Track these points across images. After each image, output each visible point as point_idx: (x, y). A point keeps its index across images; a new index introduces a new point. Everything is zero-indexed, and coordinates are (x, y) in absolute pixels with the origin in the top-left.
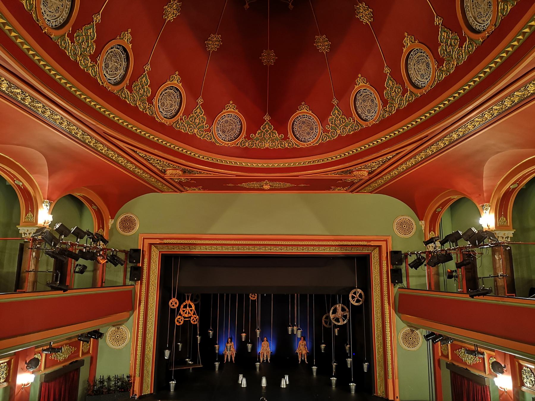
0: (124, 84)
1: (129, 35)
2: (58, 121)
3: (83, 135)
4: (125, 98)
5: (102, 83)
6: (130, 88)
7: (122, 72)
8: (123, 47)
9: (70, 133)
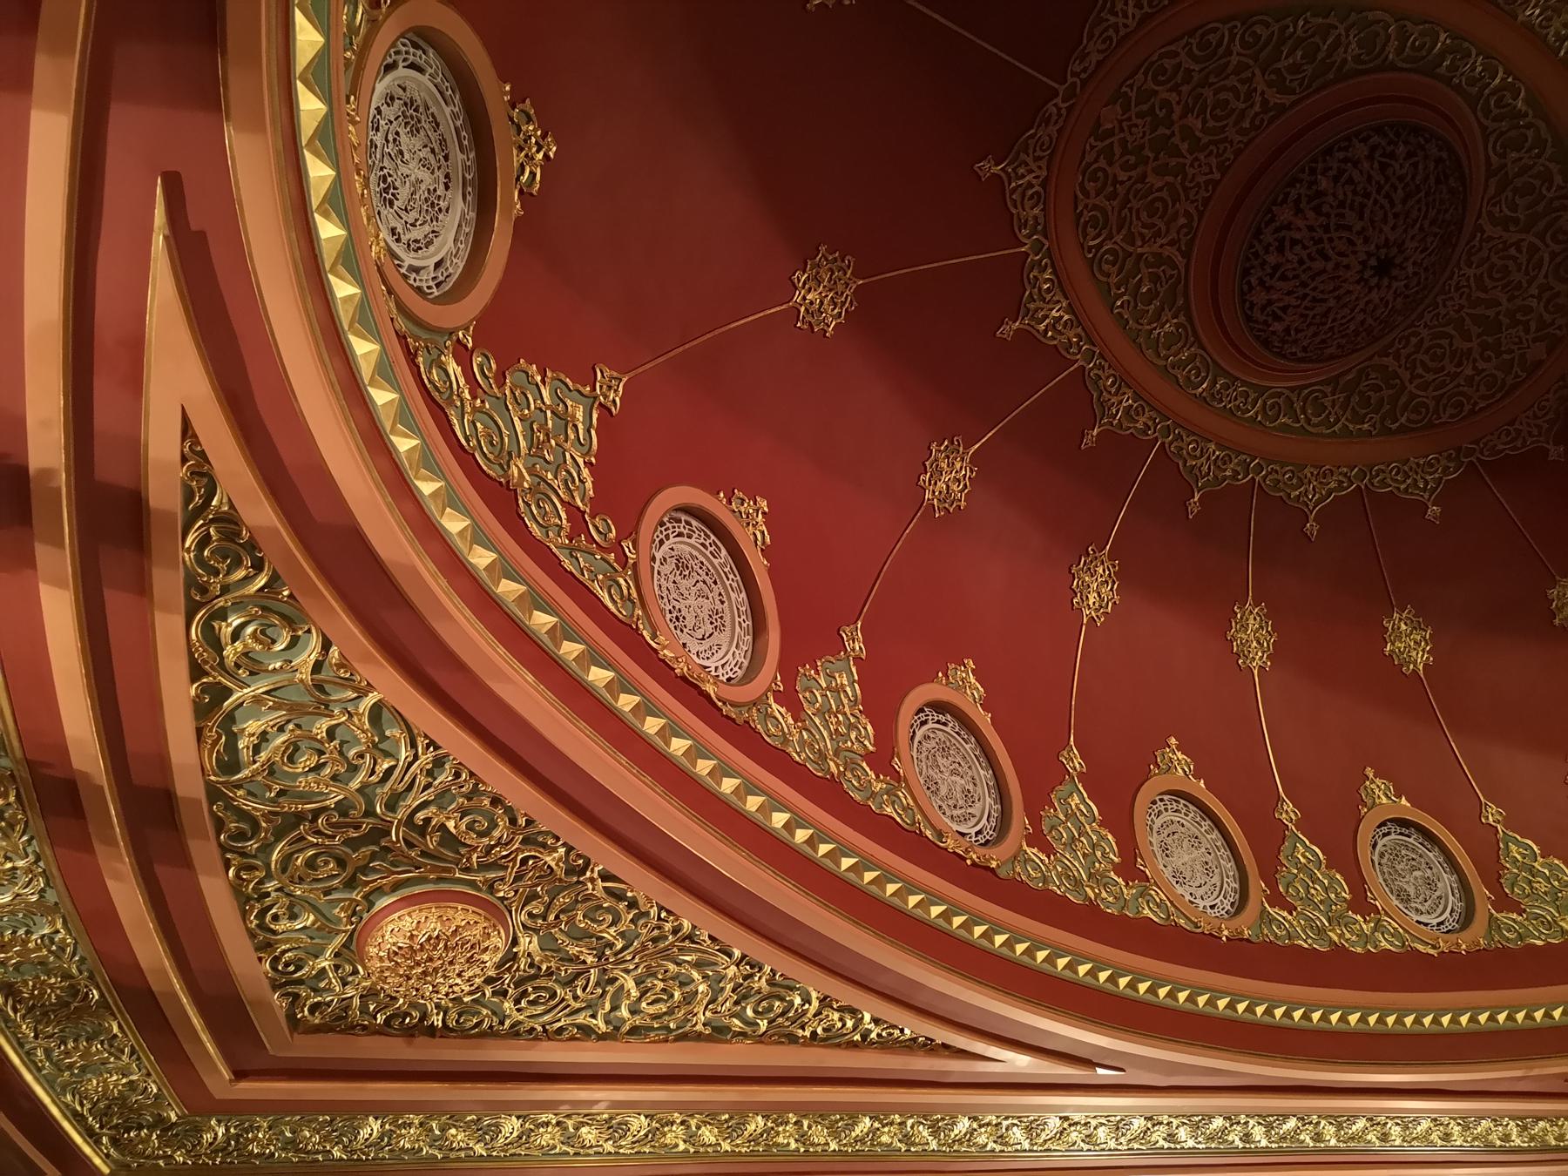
0: (1484, 908)
1: (1378, 781)
2: (1434, 1137)
3: (1524, 1128)
4: (1521, 937)
5: (1434, 947)
6: (1504, 902)
7: (1447, 880)
8: (1390, 820)
9: (1490, 1148)
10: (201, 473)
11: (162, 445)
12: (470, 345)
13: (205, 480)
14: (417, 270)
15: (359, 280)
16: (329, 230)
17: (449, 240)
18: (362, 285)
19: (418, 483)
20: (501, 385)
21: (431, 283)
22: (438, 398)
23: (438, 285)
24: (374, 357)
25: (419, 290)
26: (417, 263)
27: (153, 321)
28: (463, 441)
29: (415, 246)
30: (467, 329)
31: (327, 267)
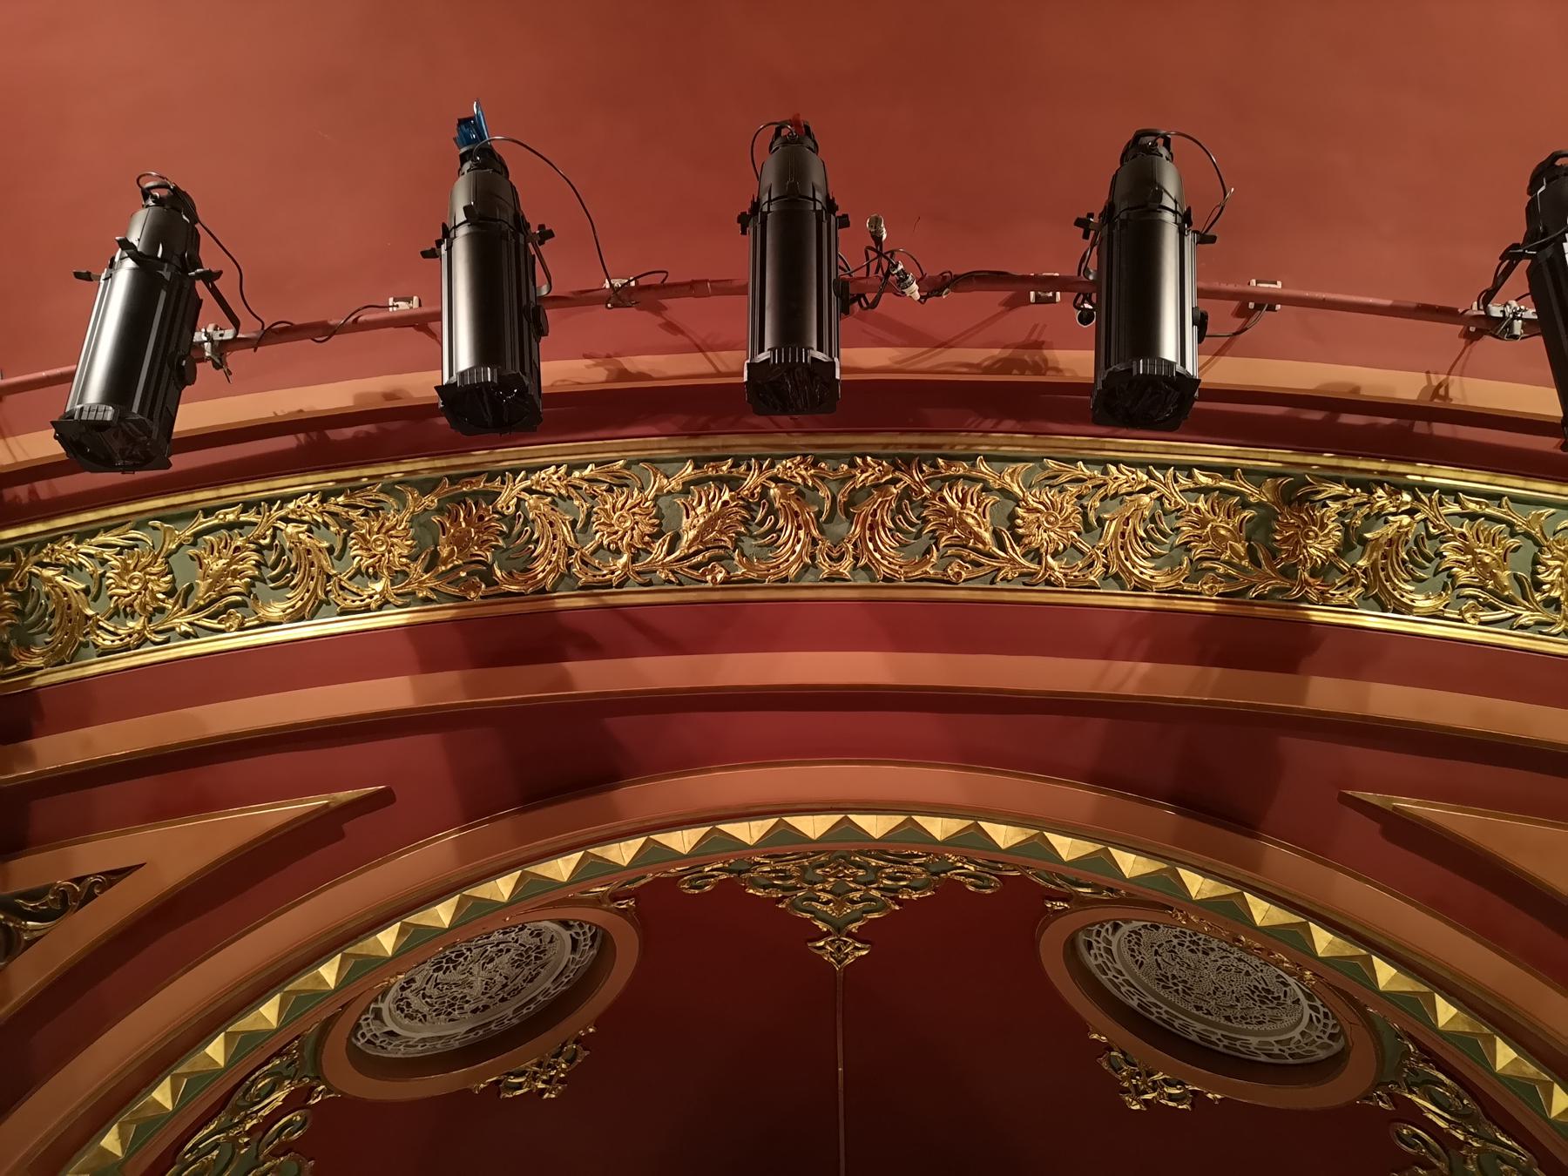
10: (64, 903)
11: (91, 856)
12: (312, 1102)
13: (59, 907)
14: (378, 1015)
15: (343, 983)
16: (387, 939)
17: (419, 1035)
18: (337, 989)
19: (115, 1128)
20: (274, 1154)
21: (368, 1036)
22: (236, 1097)
23: (369, 1042)
24: (263, 1026)
25: (358, 1026)
26: (385, 1014)
27: (236, 815)
28: (189, 1145)
29: (402, 1005)
30: (329, 1092)
31: (349, 950)
